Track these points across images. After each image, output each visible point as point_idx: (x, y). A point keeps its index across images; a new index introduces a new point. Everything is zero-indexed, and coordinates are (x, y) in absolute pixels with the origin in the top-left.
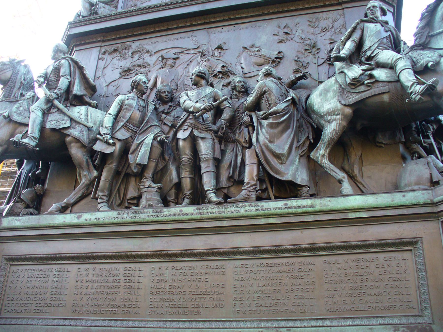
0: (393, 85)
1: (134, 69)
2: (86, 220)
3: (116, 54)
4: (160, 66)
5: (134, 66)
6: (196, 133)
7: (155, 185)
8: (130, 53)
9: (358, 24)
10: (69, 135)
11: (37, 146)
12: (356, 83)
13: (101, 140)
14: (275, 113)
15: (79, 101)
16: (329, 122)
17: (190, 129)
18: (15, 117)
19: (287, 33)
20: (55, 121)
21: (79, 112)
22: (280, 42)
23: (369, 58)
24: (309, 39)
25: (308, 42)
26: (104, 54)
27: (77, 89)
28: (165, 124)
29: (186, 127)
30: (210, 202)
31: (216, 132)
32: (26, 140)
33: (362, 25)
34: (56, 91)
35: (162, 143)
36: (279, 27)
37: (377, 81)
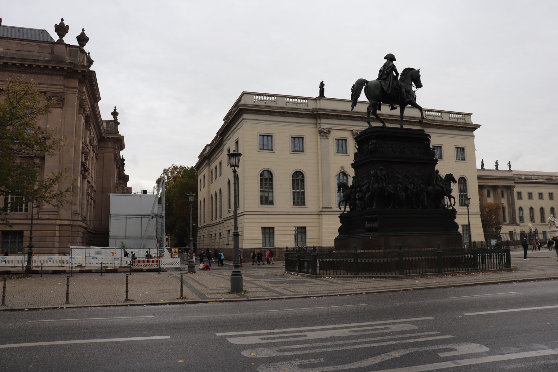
15: (389, 183)
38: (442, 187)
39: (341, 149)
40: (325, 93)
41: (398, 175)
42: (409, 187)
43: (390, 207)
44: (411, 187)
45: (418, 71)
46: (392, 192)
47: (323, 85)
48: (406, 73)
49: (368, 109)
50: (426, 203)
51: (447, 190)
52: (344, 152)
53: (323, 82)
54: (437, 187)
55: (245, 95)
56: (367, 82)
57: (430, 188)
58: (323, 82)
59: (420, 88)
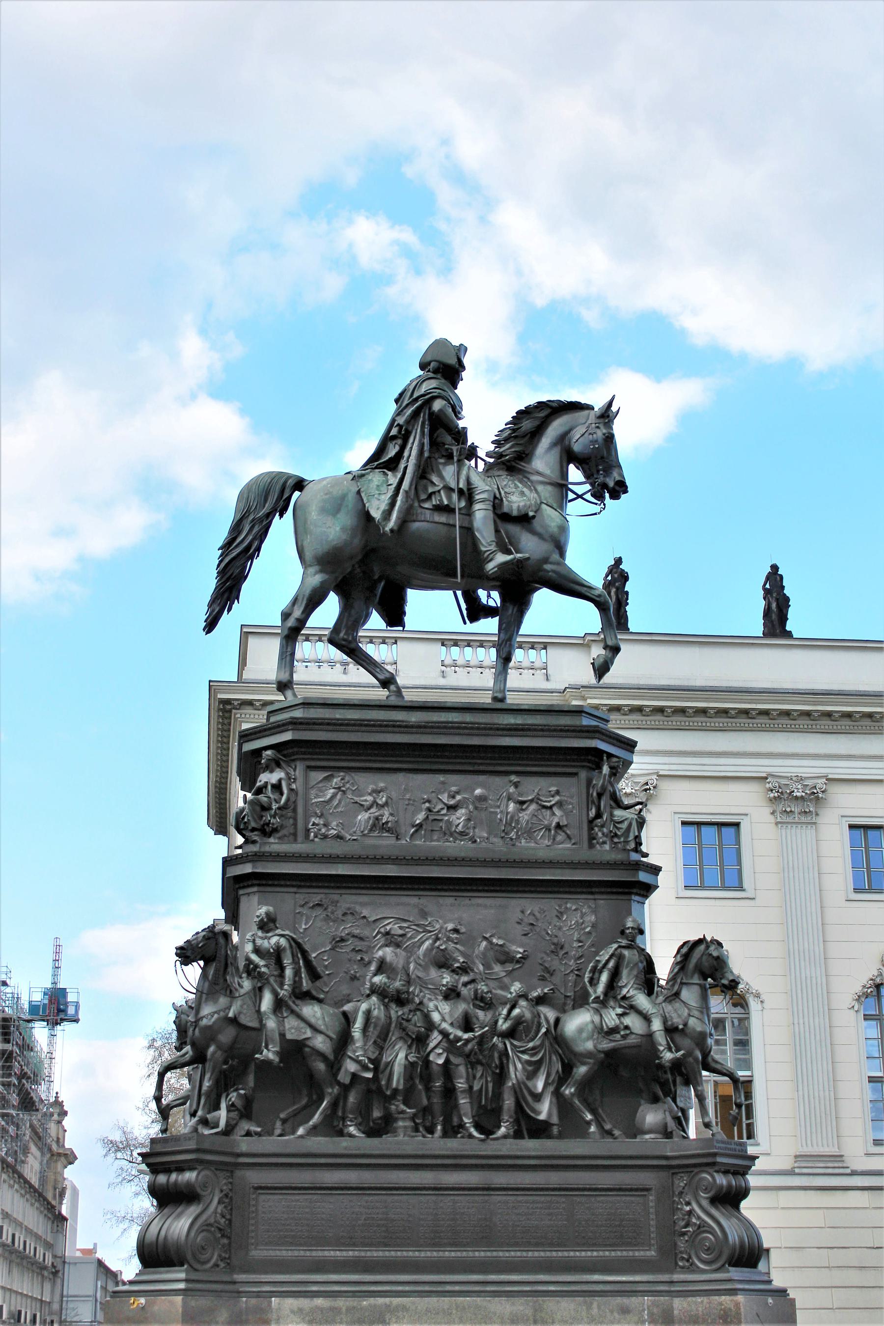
0: (644, 1039)
1: (348, 940)
2: (346, 1148)
3: (319, 911)
4: (382, 941)
5: (348, 934)
6: (453, 1059)
7: (408, 1110)
8: (339, 913)
9: (616, 949)
10: (309, 1047)
11: (281, 1061)
12: (614, 1031)
13: (350, 1058)
14: (533, 1048)
15: (306, 996)
16: (584, 1064)
17: (445, 1055)
18: (243, 1020)
19: (532, 924)
20: (293, 1029)
21: (311, 1011)
22: (525, 935)
23: (624, 998)
24: (556, 936)
25: (555, 940)
26: (302, 906)
27: (306, 984)
28: (407, 1034)
29: (441, 1051)
30: (471, 1136)
31: (468, 1056)
32: (271, 1056)
33: (619, 950)
34: (286, 987)
35: (412, 1065)
36: (523, 912)
37: (632, 1033)
38: (647, 1018)
39: (713, 874)
40: (631, 610)
41: (388, 953)
42: (436, 1017)
43: (301, 1131)
44: (442, 1013)
45: (607, 415)
46: (320, 1043)
47: (625, 577)
48: (527, 425)
49: (285, 616)
50: (545, 1110)
51: (670, 1030)
52: (731, 881)
53: (619, 561)
54: (611, 1017)
55: (252, 641)
56: (300, 485)
57: (578, 1022)
58: (619, 561)
59: (615, 496)
